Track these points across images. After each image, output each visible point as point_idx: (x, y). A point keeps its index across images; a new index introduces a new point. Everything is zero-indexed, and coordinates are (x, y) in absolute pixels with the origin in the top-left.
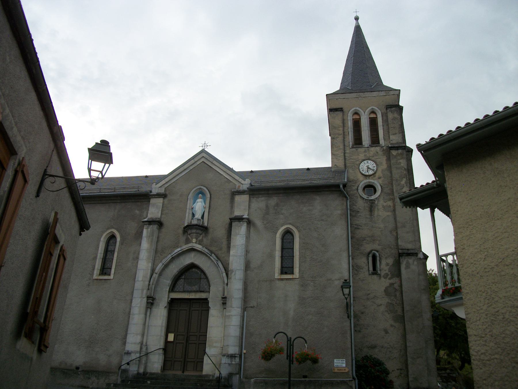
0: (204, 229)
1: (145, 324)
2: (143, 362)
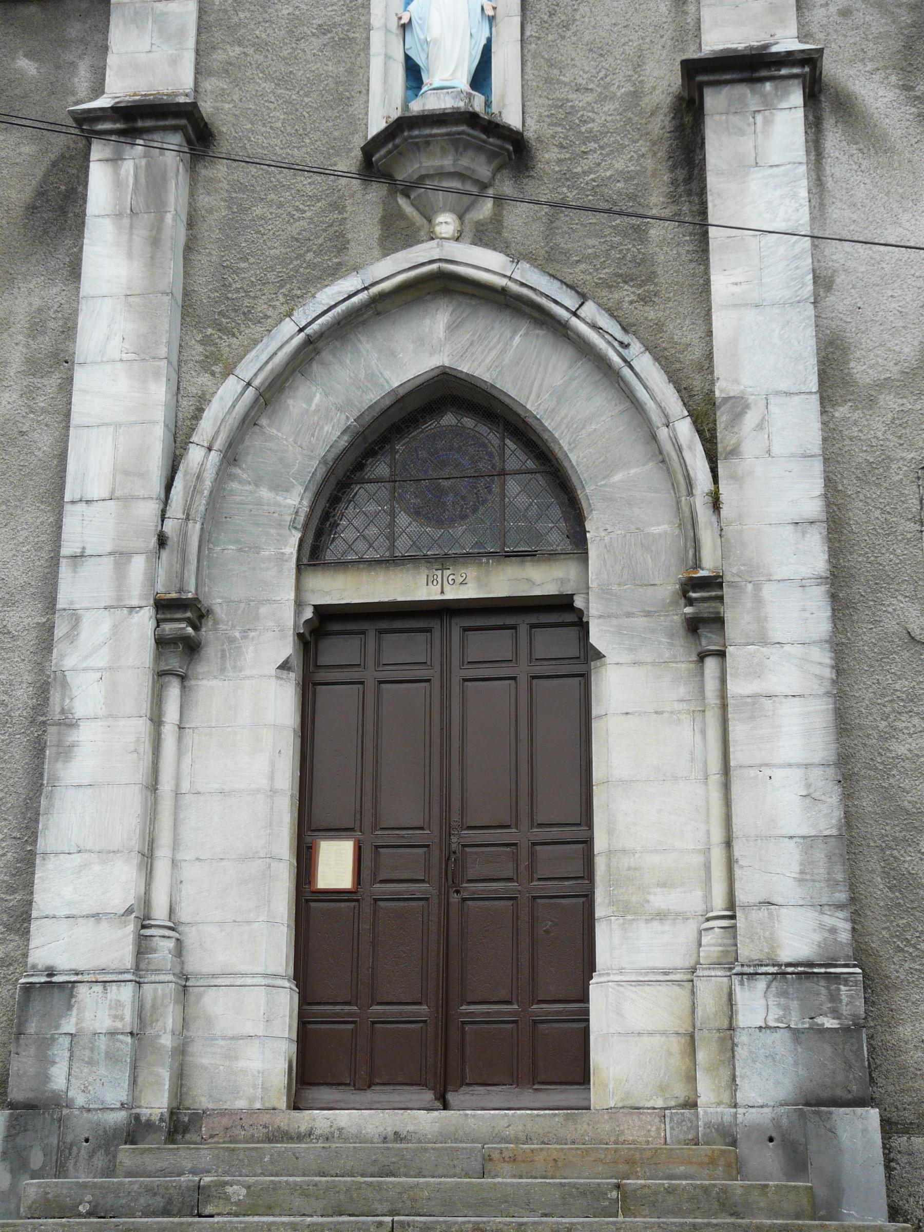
0: (513, 150)
1: (153, 786)
2: (167, 1041)
